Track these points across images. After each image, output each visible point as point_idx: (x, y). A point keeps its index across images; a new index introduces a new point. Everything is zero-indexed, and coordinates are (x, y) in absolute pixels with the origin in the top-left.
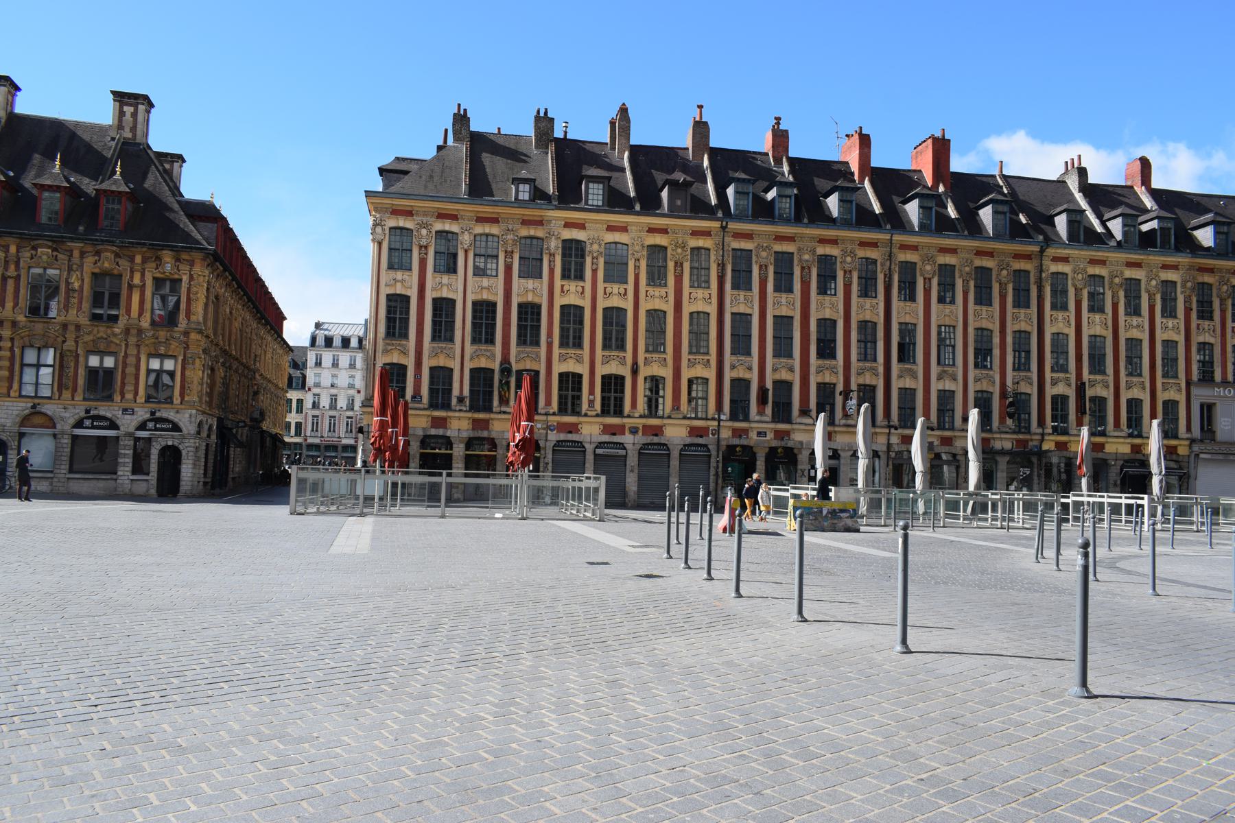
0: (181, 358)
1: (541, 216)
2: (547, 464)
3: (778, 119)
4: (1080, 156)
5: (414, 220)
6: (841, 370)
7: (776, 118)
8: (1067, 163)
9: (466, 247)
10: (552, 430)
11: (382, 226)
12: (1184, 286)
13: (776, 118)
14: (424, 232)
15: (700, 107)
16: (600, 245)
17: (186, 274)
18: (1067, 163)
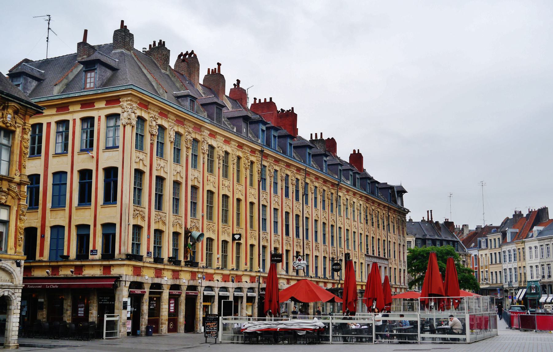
0: (15, 209)
1: (201, 126)
2: (201, 303)
3: (238, 81)
4: (321, 133)
5: (149, 113)
6: (291, 242)
7: (238, 80)
8: (311, 134)
9: (172, 140)
10: (204, 279)
11: (135, 113)
12: (363, 207)
13: (238, 80)
14: (154, 123)
15: (219, 64)
16: (223, 152)
17: (19, 127)
18: (311, 134)
